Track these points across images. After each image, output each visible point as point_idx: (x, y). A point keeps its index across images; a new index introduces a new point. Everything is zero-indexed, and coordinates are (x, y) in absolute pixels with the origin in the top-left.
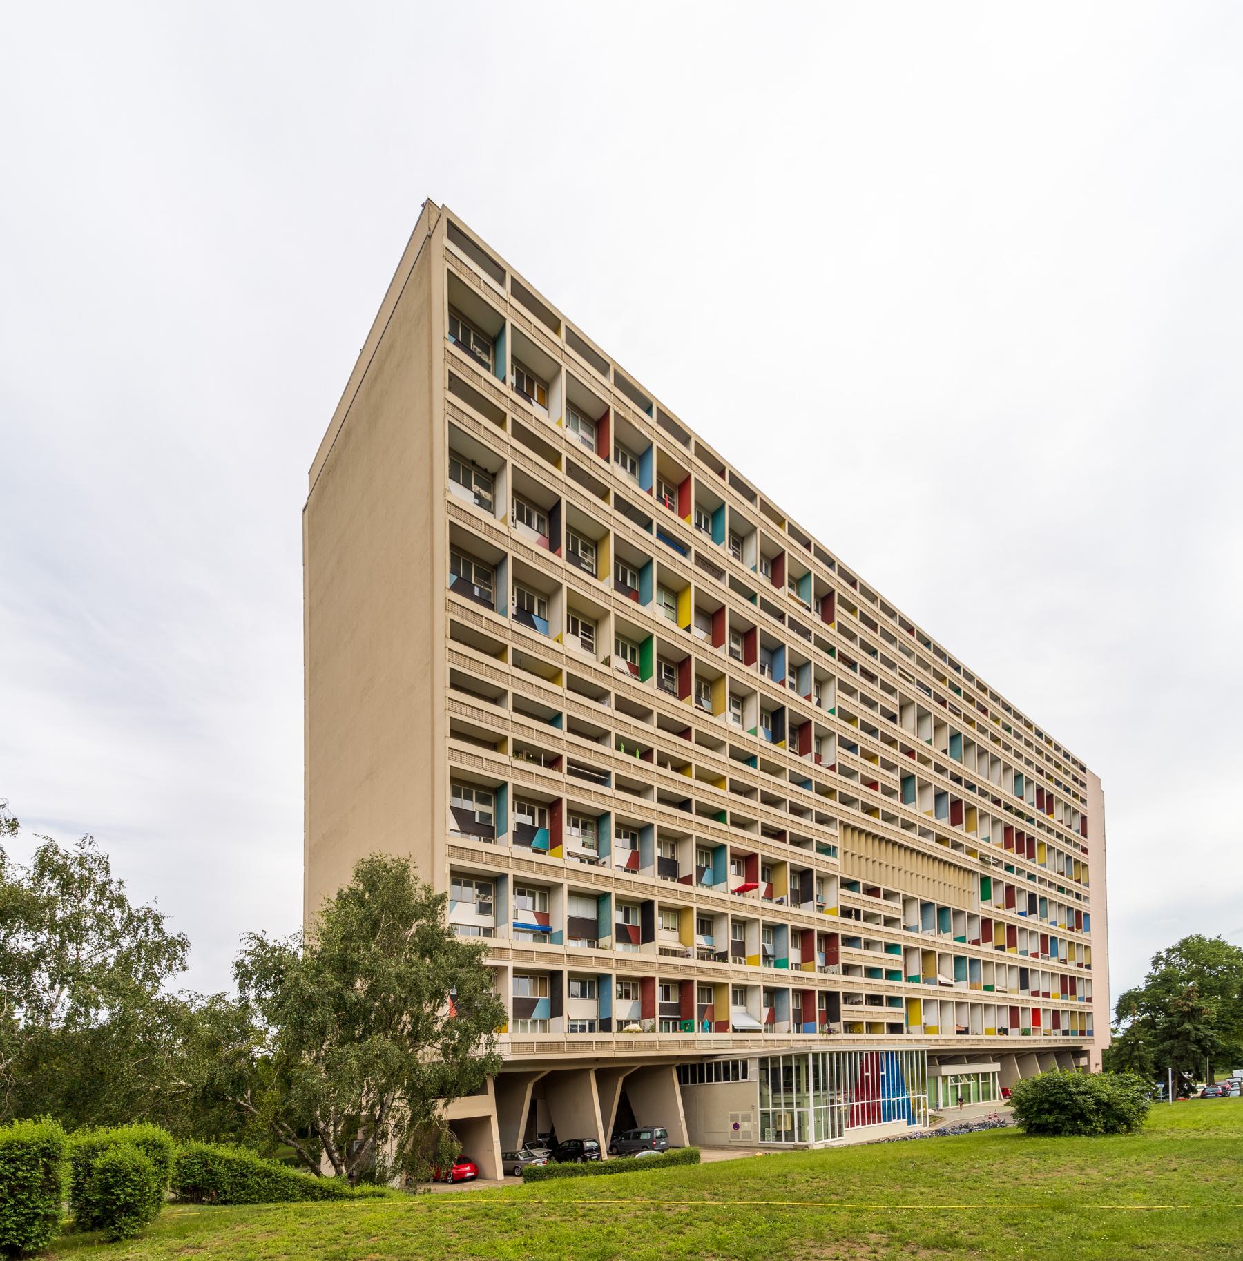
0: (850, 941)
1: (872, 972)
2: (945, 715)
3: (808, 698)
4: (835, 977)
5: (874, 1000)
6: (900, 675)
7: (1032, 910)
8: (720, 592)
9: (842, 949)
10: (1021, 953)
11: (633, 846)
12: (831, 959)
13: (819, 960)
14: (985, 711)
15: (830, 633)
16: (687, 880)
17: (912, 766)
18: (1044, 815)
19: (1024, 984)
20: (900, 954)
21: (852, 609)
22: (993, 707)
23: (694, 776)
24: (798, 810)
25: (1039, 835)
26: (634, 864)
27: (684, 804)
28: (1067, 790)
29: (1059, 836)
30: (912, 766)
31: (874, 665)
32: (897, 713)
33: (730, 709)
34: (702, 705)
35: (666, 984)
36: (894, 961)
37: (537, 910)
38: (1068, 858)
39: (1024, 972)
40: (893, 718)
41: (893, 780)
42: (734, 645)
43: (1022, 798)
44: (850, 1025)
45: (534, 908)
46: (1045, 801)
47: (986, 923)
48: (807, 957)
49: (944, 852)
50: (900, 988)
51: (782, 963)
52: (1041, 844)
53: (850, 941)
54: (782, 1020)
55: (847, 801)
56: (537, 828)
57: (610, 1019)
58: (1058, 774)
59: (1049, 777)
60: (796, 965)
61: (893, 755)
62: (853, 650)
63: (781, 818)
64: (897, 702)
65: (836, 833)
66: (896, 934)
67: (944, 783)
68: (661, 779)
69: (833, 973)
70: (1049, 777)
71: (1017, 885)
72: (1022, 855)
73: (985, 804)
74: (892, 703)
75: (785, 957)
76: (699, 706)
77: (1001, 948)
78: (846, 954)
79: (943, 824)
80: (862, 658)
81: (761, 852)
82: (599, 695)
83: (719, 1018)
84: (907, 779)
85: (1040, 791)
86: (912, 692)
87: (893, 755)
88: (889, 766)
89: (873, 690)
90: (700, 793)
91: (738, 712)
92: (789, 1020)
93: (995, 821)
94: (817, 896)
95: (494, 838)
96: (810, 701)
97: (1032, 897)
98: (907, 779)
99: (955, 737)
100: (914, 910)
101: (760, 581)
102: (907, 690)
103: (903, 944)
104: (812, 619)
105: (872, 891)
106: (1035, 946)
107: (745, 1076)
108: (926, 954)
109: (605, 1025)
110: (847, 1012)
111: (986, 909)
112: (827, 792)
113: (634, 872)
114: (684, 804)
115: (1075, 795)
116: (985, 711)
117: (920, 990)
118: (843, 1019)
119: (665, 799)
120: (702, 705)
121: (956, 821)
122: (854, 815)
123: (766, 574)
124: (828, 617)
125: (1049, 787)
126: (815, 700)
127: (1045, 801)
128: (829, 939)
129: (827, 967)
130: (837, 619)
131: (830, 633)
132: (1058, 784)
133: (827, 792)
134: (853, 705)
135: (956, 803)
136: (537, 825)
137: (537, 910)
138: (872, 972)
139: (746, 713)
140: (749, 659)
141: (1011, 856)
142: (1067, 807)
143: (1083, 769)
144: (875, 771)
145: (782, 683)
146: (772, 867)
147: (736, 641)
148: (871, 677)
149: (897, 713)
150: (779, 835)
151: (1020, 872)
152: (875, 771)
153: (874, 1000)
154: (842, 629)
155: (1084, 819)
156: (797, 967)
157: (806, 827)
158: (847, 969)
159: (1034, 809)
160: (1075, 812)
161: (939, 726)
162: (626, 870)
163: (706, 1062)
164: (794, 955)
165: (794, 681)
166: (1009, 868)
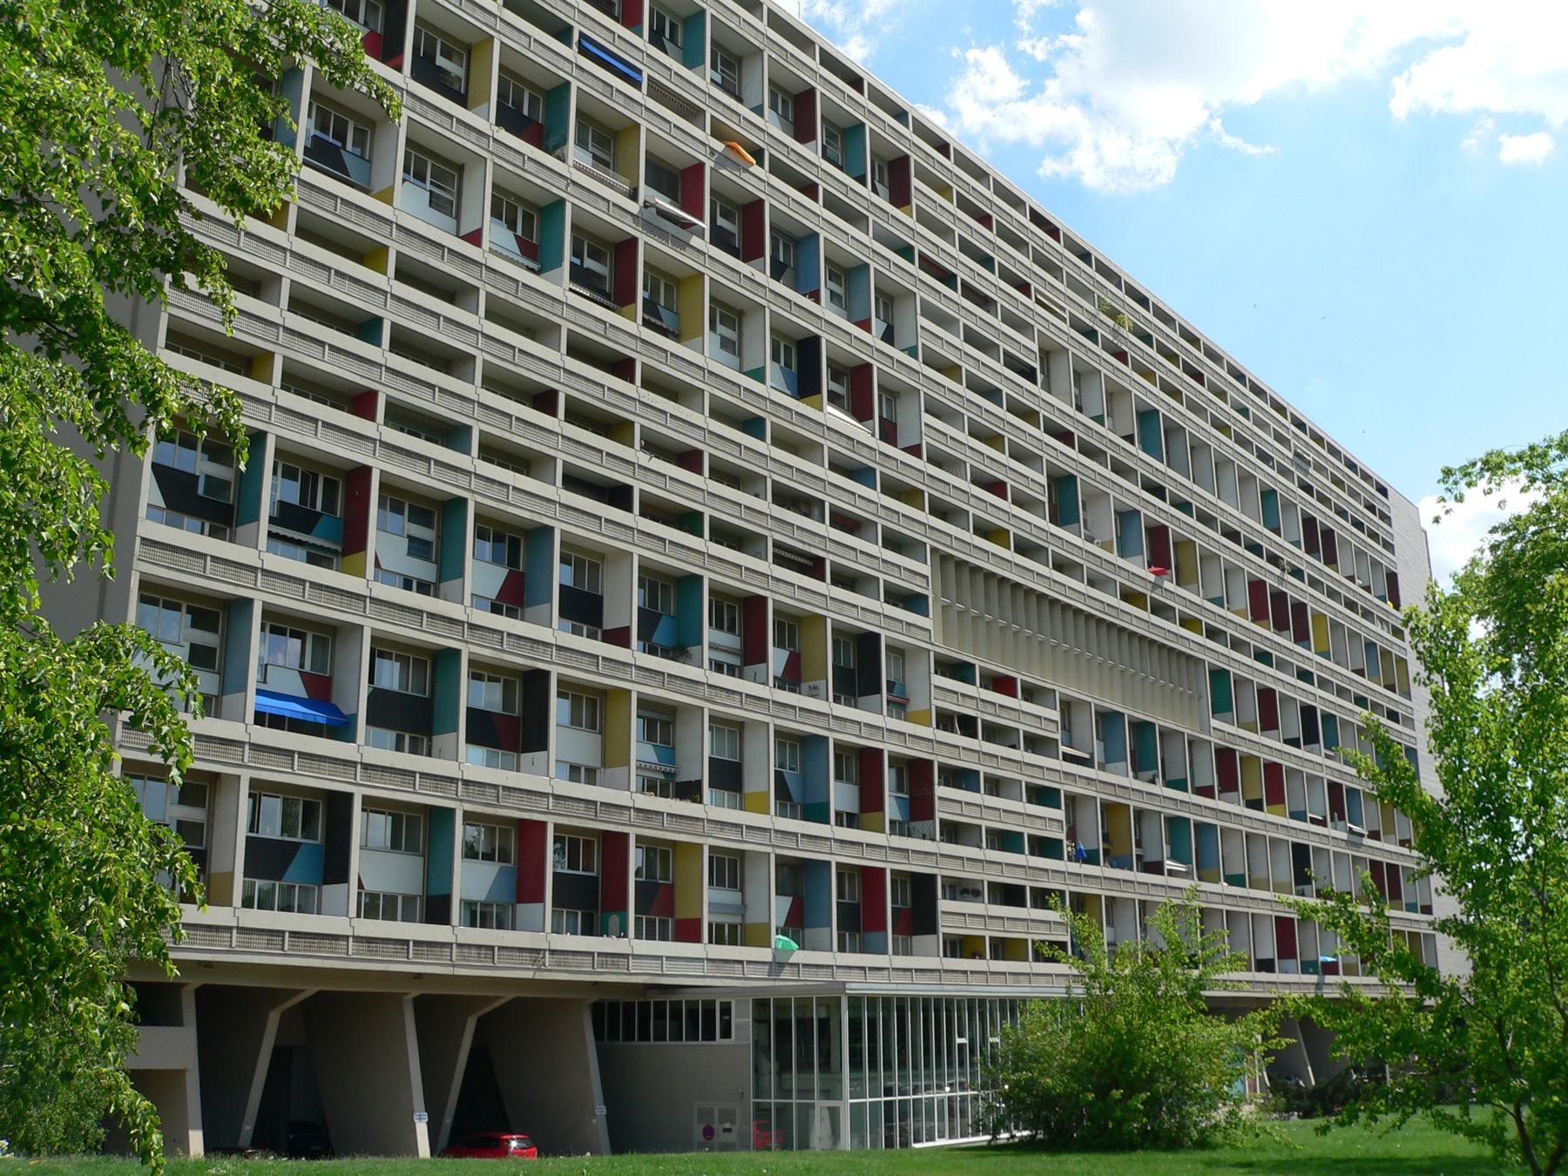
0: (959, 777)
1: (1005, 840)
2: (1127, 376)
3: (865, 325)
4: (926, 846)
5: (1010, 895)
6: (1038, 302)
7: (1310, 737)
8: (696, 143)
9: (941, 791)
10: (1294, 815)
11: (513, 562)
12: (919, 808)
13: (891, 808)
14: (1198, 377)
15: (904, 222)
16: (619, 637)
17: (1069, 458)
18: (1320, 565)
19: (1302, 878)
20: (1059, 808)
21: (944, 189)
22: (1208, 367)
23: (637, 445)
24: (847, 522)
25: (1315, 601)
26: (513, 599)
27: (618, 495)
28: (1358, 525)
29: (1351, 605)
30: (1069, 458)
31: (988, 282)
32: (1037, 366)
33: (713, 328)
34: (661, 320)
35: (571, 841)
36: (1049, 821)
37: (307, 668)
38: (1370, 646)
39: (1301, 853)
40: (1029, 374)
41: (1035, 481)
42: (721, 221)
43: (1277, 531)
44: (961, 941)
45: (302, 666)
46: (1319, 541)
47: (1225, 757)
48: (871, 801)
49: (1137, 619)
50: (1062, 873)
51: (817, 812)
52: (1319, 616)
53: (959, 777)
54: (815, 925)
55: (943, 511)
56: (319, 515)
57: (446, 900)
58: (1340, 496)
59: (1323, 499)
60: (848, 814)
61: (1033, 436)
62: (949, 255)
63: (816, 534)
64: (1036, 349)
65: (925, 569)
66: (1050, 769)
67: (1132, 494)
68: (572, 448)
69: (924, 837)
70: (1323, 499)
71: (1278, 688)
72: (1285, 633)
73: (1208, 539)
74: (1027, 349)
75: (825, 800)
76: (653, 320)
77: (1255, 804)
78: (949, 801)
79: (1137, 569)
80: (966, 269)
81: (774, 597)
82: (453, 292)
83: (682, 913)
84: (1062, 483)
85: (1309, 522)
86: (1062, 334)
87: (1033, 436)
88: (1020, 455)
89: (989, 323)
90: (651, 478)
91: (731, 334)
92: (831, 926)
93: (1230, 571)
94: (891, 685)
95: (230, 525)
96: (869, 330)
97: (1308, 712)
98: (1062, 483)
99: (1147, 416)
100: (1087, 726)
101: (771, 129)
102: (1052, 328)
103: (1065, 787)
104: (871, 198)
105: (1003, 684)
106: (1320, 804)
107: (726, 1033)
108: (1108, 808)
109: (437, 911)
110: (953, 914)
111: (1223, 731)
112: (908, 494)
113: (512, 614)
114: (618, 495)
115: (1373, 536)
116: (1198, 377)
117: (1099, 878)
118: (942, 930)
119: (576, 481)
120: (661, 320)
121: (1159, 560)
122: (960, 539)
123: (784, 116)
124: (900, 196)
125: (1325, 517)
126: (877, 326)
127: (1319, 541)
128: (916, 774)
129: (914, 824)
130: (914, 201)
131: (904, 222)
132: (1342, 513)
133: (908, 494)
134: (952, 345)
135: (1158, 534)
136: (319, 508)
137: (307, 668)
138: (1005, 840)
139: (746, 338)
140: (749, 251)
141: (1265, 634)
142: (1360, 553)
143: (1383, 491)
144: (999, 463)
145: (815, 296)
146: (794, 626)
147: (727, 215)
148: (984, 302)
149: (1037, 366)
150: (812, 566)
151: (1282, 665)
152: (999, 463)
153: (1010, 895)
154: (925, 219)
155: (1392, 578)
156: (850, 820)
157: (865, 553)
158: (953, 832)
159: (1301, 553)
160: (1375, 563)
161: (1115, 394)
162: (496, 609)
163: (653, 999)
164: (841, 796)
165: (839, 290)
166: (1262, 656)
